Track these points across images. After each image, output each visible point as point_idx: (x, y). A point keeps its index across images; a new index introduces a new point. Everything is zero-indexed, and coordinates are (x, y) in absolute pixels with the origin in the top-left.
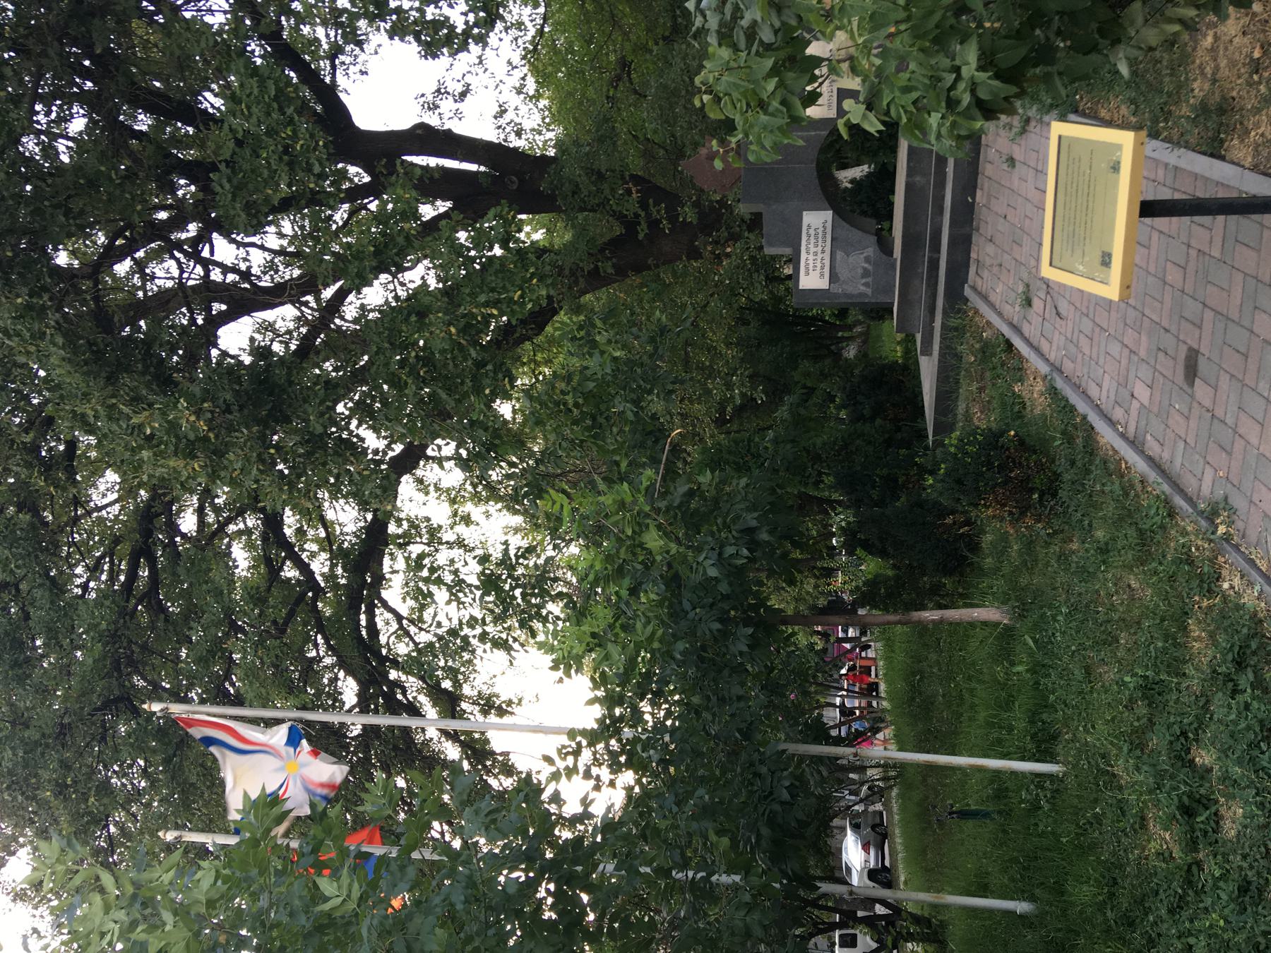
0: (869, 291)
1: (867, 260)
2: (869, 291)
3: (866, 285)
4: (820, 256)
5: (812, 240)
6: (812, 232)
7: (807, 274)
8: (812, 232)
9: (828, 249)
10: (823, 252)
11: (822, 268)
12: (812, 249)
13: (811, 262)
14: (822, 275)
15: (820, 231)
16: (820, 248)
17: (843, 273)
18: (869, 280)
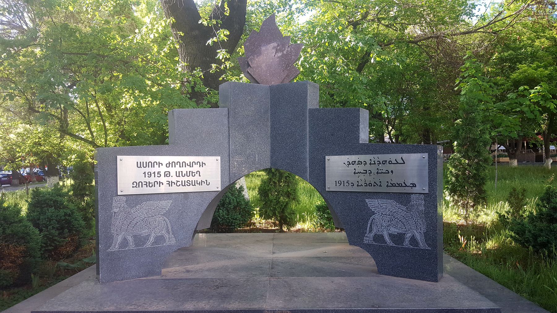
0: (115, 247)
1: (160, 239)
2: (115, 247)
3: (125, 242)
4: (163, 179)
5: (185, 170)
6: (196, 168)
7: (140, 165)
8: (196, 168)
9: (174, 189)
10: (170, 184)
11: (148, 184)
12: (173, 170)
13: (156, 169)
14: (137, 184)
15: (197, 178)
16: (174, 179)
18: (132, 246)
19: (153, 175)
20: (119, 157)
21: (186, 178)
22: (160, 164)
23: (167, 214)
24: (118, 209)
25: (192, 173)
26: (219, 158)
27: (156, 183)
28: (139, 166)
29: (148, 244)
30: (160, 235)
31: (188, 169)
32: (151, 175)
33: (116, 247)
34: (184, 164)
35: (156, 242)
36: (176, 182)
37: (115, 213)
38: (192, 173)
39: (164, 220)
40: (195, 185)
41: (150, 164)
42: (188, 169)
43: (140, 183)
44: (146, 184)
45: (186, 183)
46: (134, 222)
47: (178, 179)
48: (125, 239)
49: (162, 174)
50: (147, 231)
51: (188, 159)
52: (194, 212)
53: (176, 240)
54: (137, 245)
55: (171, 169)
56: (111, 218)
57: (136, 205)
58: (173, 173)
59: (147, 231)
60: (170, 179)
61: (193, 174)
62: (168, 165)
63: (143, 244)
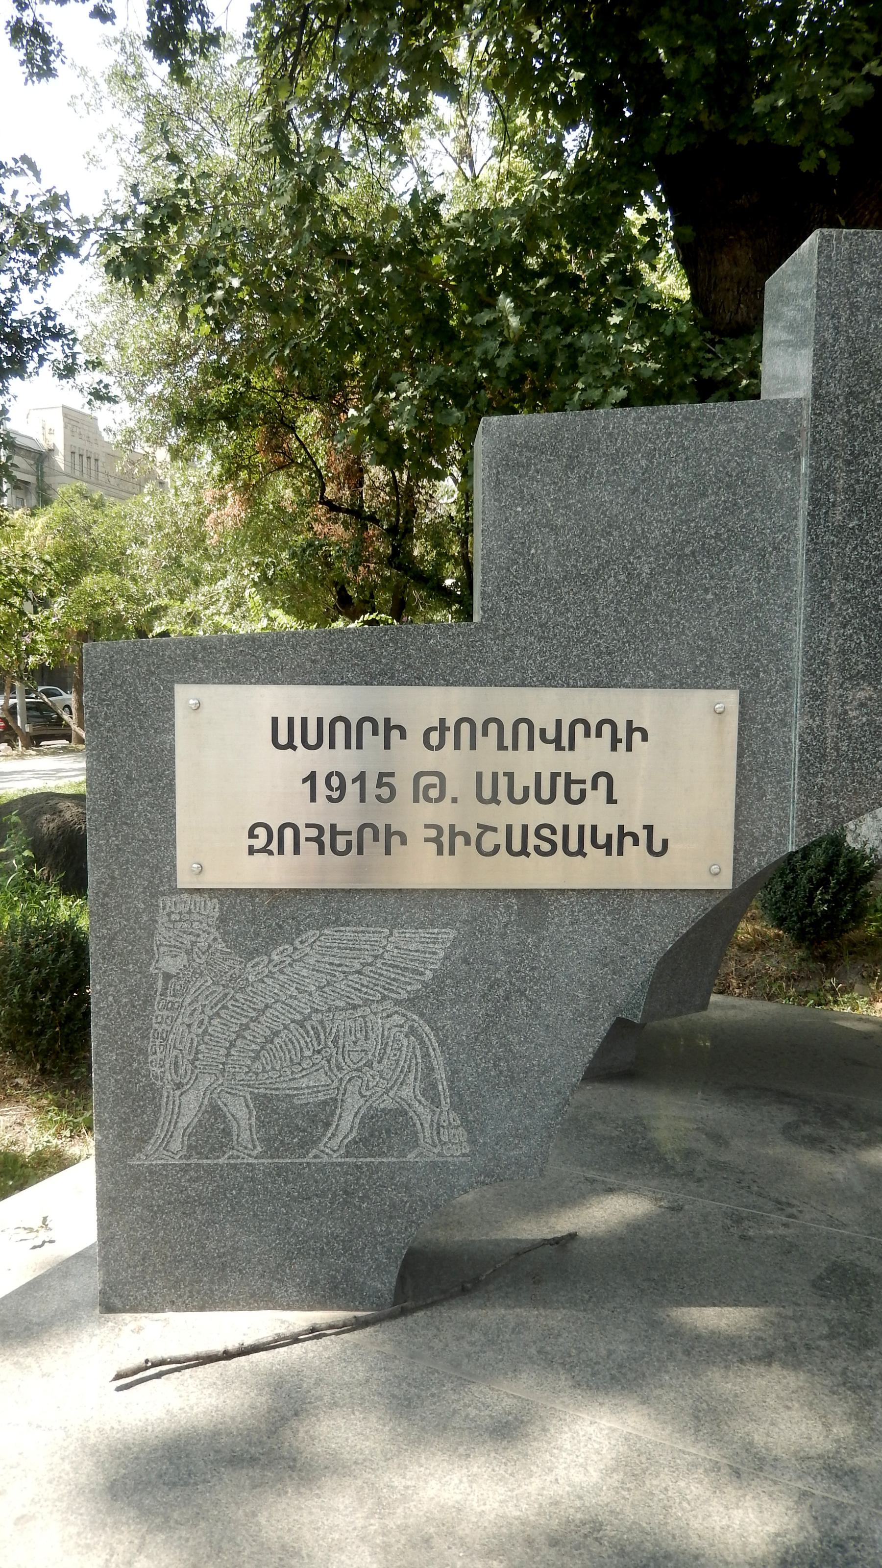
1: (384, 1128)
3: (213, 1129)
6: (589, 756)
7: (286, 736)
8: (589, 756)
14: (271, 839)
15: (594, 812)
16: (467, 814)
17: (298, 974)
18: (247, 1147)
19: (352, 790)
20: (185, 695)
21: (534, 814)
22: (390, 730)
23: (425, 1002)
24: (182, 960)
25: (569, 781)
26: (729, 699)
27: (368, 833)
28: (283, 739)
29: (332, 1147)
30: (387, 1103)
31: (546, 760)
32: (342, 788)
33: (176, 1146)
34: (523, 733)
35: (365, 1141)
36: (474, 833)
37: (167, 977)
38: (569, 781)
39: (412, 1031)
40: (581, 852)
41: (340, 727)
42: (546, 760)
43: (289, 833)
44: (318, 840)
45: (532, 840)
46: (261, 1030)
47: (490, 814)
48: (214, 1111)
49: (404, 786)
50: (324, 1080)
51: (547, 705)
52: (574, 998)
53: (472, 1142)
54: (271, 1146)
55: (449, 760)
56: (148, 1001)
57: (272, 942)
58: (459, 783)
59: (324, 1080)
60: (443, 814)
61: (575, 794)
62: (434, 738)
63: (307, 1144)
